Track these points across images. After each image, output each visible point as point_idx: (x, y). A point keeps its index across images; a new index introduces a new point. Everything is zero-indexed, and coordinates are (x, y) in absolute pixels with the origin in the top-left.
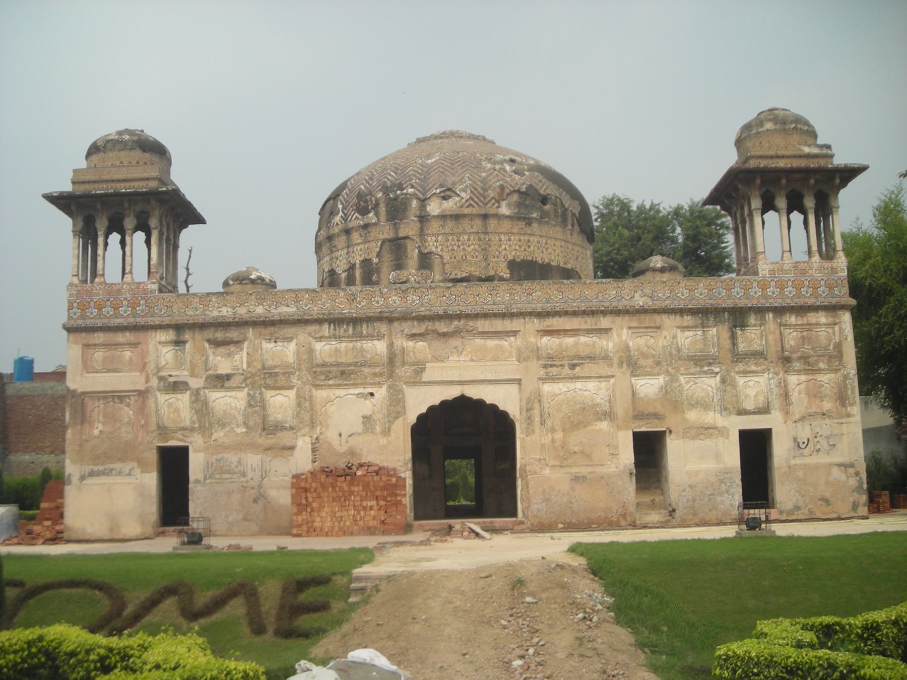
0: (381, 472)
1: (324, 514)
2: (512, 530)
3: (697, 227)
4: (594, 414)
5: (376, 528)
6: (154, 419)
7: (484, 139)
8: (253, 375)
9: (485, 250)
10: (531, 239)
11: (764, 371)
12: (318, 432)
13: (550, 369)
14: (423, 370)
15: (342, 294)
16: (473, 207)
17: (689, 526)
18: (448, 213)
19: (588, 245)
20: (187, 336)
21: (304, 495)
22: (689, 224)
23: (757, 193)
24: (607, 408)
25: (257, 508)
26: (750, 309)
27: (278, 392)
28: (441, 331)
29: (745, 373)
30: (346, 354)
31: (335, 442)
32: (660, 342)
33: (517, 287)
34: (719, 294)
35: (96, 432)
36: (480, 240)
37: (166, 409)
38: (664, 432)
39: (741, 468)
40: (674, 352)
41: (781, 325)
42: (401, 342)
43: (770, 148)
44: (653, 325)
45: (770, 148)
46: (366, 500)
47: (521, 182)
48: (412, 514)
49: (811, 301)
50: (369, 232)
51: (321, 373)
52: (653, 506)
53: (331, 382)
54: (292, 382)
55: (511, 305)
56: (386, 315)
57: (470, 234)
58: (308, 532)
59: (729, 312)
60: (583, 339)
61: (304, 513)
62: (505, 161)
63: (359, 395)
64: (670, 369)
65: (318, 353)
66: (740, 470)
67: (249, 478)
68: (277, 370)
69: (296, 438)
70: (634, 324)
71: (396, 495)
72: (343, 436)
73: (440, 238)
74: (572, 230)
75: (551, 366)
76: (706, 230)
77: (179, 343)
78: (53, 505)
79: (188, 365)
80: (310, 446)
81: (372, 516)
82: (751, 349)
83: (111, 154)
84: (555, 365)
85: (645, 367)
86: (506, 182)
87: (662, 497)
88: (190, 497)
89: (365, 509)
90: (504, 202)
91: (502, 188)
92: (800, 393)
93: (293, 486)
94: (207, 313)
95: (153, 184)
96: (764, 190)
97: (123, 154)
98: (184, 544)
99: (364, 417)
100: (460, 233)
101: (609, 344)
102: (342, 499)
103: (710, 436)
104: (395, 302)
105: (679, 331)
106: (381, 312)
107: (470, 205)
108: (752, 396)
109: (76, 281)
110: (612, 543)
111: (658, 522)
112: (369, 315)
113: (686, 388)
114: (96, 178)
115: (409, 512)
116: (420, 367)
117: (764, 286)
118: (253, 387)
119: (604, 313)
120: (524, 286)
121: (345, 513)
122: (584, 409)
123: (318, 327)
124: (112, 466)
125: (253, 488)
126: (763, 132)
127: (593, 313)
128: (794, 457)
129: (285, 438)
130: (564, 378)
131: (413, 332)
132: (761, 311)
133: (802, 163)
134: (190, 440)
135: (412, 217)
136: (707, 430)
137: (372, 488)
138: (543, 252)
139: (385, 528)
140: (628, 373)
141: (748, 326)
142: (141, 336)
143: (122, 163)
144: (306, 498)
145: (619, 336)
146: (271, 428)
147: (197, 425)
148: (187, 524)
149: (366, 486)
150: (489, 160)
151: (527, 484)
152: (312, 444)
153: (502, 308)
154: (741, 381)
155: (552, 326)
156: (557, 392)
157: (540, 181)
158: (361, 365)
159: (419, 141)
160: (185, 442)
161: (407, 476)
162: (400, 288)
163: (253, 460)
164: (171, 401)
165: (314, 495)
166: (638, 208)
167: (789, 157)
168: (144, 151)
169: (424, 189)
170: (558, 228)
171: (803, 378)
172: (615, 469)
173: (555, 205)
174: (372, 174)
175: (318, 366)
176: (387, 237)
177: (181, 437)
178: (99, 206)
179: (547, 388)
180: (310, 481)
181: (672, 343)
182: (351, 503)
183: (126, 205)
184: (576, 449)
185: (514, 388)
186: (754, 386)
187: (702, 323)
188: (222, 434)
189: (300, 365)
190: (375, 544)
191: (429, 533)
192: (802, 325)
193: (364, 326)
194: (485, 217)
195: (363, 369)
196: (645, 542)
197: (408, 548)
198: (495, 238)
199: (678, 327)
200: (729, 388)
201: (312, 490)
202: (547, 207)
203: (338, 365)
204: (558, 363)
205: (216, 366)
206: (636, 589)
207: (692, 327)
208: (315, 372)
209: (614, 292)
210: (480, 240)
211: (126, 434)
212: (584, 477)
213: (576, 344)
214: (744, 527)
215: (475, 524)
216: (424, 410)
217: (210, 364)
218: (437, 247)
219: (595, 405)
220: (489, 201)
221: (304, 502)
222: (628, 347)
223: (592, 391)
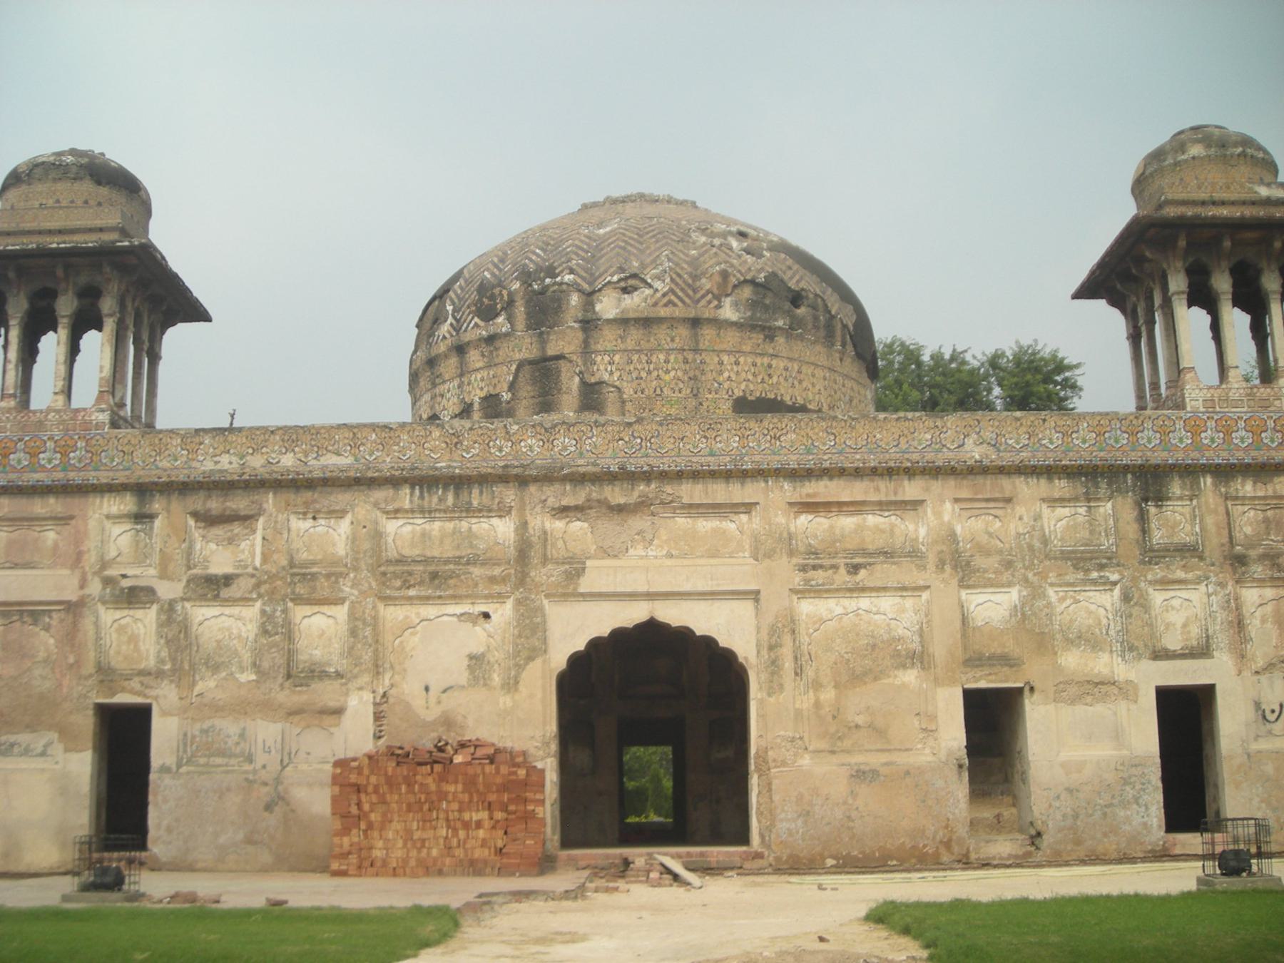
0: (499, 758)
1: (390, 835)
2: (741, 870)
3: (1028, 384)
4: (892, 657)
5: (485, 862)
6: (92, 655)
8: (272, 577)
9: (694, 378)
10: (774, 362)
11: (1198, 581)
12: (387, 682)
13: (811, 573)
14: (580, 572)
15: (436, 433)
16: (675, 305)
17: (1067, 864)
18: (632, 315)
19: (868, 381)
20: (157, 505)
21: (354, 798)
22: (1015, 380)
23: (1179, 264)
24: (915, 645)
25: (272, 820)
26: (1173, 467)
27: (316, 608)
28: (614, 502)
29: (1165, 583)
30: (442, 542)
31: (418, 702)
32: (1012, 526)
33: (752, 424)
34: (1117, 441)
36: (686, 361)
37: (114, 636)
38: (1019, 691)
39: (1162, 756)
40: (1037, 544)
41: (1226, 498)
42: (541, 522)
43: (1199, 188)
44: (997, 495)
45: (1199, 188)
46: (470, 810)
47: (759, 267)
48: (557, 837)
50: (496, 349)
51: (396, 575)
52: (998, 825)
53: (412, 592)
54: (342, 591)
55: (742, 456)
56: (515, 471)
57: (668, 351)
58: (359, 867)
59: (1134, 474)
60: (872, 520)
61: (354, 831)
62: (730, 233)
63: (462, 617)
64: (1030, 575)
65: (390, 540)
66: (1158, 760)
67: (258, 766)
68: (315, 570)
69: (347, 694)
70: (965, 494)
71: (526, 801)
72: (431, 693)
73: (617, 358)
74: (842, 353)
75: (815, 568)
76: (1041, 388)
77: (143, 517)
79: (156, 558)
80: (371, 709)
81: (481, 840)
82: (1176, 540)
83: (39, 187)
84: (821, 567)
85: (986, 571)
86: (732, 266)
87: (1014, 810)
88: (151, 798)
89: (466, 825)
90: (728, 300)
91: (725, 275)
92: (1263, 621)
93: (335, 780)
94: (195, 464)
95: (107, 237)
96: (1191, 260)
97: (60, 186)
98: (86, 888)
99: (471, 657)
100: (652, 351)
101: (919, 529)
102: (426, 807)
103: (1104, 698)
105: (1044, 506)
106: (506, 466)
107: (670, 302)
108: (1179, 625)
110: (958, 905)
111: (1010, 856)
112: (484, 471)
113: (1059, 610)
114: (12, 227)
115: (551, 833)
116: (575, 568)
117: (1195, 428)
118: (271, 600)
119: (910, 473)
120: (766, 423)
121: (430, 833)
122: (874, 646)
123: (391, 492)
124: (12, 738)
125: (266, 784)
126: (1186, 161)
128: (1257, 737)
129: (326, 693)
130: (837, 590)
131: (565, 502)
132: (1190, 472)
133: (1261, 212)
134: (153, 693)
137: (481, 788)
138: (793, 386)
140: (955, 582)
141: (1169, 499)
143: (58, 201)
144: (359, 805)
145: (938, 514)
146: (300, 674)
147: (168, 667)
148: (142, 846)
149: (470, 784)
150: (703, 231)
151: (770, 784)
152: (376, 704)
153: (725, 462)
154: (1158, 598)
155: (815, 495)
156: (825, 615)
157: (790, 268)
158: (468, 563)
159: (585, 207)
160: (145, 696)
161: (549, 767)
162: (541, 425)
163: (266, 731)
164: (123, 622)
165: (374, 798)
166: (932, 357)
167: (1233, 203)
168: (99, 183)
169: (592, 275)
170: (819, 348)
171: (1269, 593)
172: (930, 758)
173: (814, 308)
174: (505, 254)
175: (389, 562)
176: (525, 354)
177: (138, 687)
178: (11, 275)
179: (807, 608)
180: (366, 771)
181: (1033, 528)
182: (442, 815)
183: (60, 272)
184: (860, 720)
185: (745, 609)
187: (1087, 493)
188: (212, 684)
189: (356, 560)
190: (470, 897)
191: (587, 873)
192: (1265, 498)
193: (476, 492)
194: (695, 323)
195: (471, 569)
196: (1024, 902)
197: (539, 904)
198: (712, 360)
199: (1043, 500)
200: (1136, 611)
201: (370, 789)
202: (802, 311)
203: (426, 561)
204: (827, 562)
205: (206, 560)
207: (1069, 500)
208: (384, 574)
209: (928, 436)
210: (686, 361)
211: (41, 681)
212: (875, 773)
213: (860, 528)
214: (1212, 867)
215: (673, 857)
216: (580, 645)
217: (196, 556)
218: (611, 373)
219: (894, 639)
220: (703, 297)
221: (354, 810)
222: (952, 536)
223: (888, 613)
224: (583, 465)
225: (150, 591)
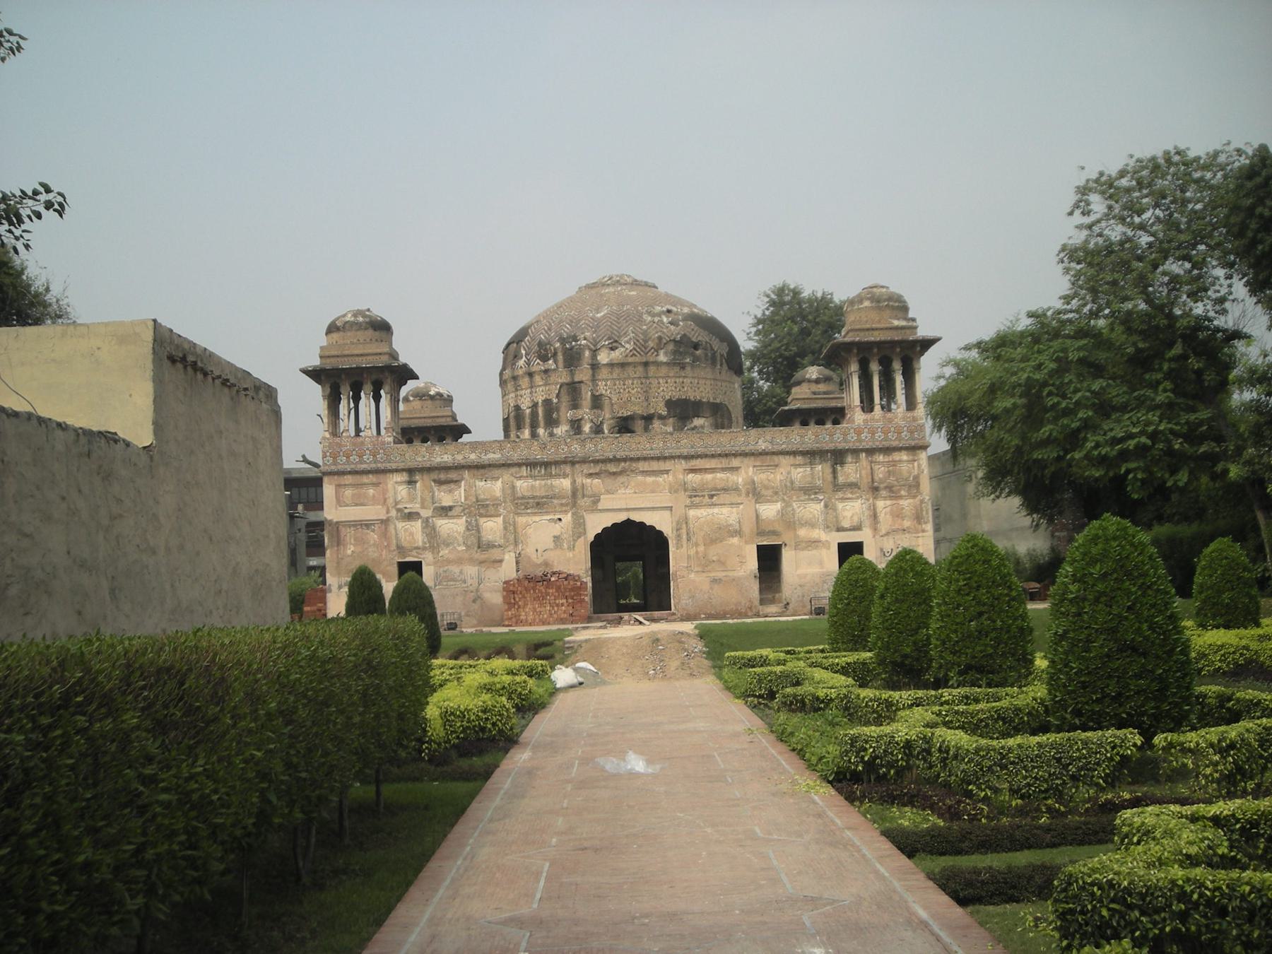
2: (667, 620)
7: (646, 284)
8: (470, 507)
25: (476, 606)
29: (843, 499)
31: (534, 557)
35: (349, 552)
42: (580, 480)
49: (895, 444)
60: (719, 475)
77: (411, 482)
78: (314, 608)
81: (563, 611)
91: (660, 338)
93: (504, 589)
97: (359, 333)
102: (541, 599)
104: (576, 448)
109: (327, 435)
116: (596, 502)
119: (735, 455)
127: (726, 455)
129: (495, 554)
135: (586, 366)
136: (814, 544)
139: (572, 618)
142: (381, 477)
145: (747, 473)
146: (483, 546)
149: (558, 589)
150: (649, 313)
153: (657, 453)
154: (840, 506)
159: (591, 287)
161: (588, 580)
163: (471, 571)
170: (708, 369)
171: (888, 502)
179: (692, 513)
185: (668, 513)
186: (852, 509)
194: (646, 364)
198: (655, 382)
203: (534, 498)
206: (722, 644)
211: (372, 553)
213: (714, 479)
222: (753, 482)
223: (726, 514)
224: (597, 456)
225: (418, 514)
